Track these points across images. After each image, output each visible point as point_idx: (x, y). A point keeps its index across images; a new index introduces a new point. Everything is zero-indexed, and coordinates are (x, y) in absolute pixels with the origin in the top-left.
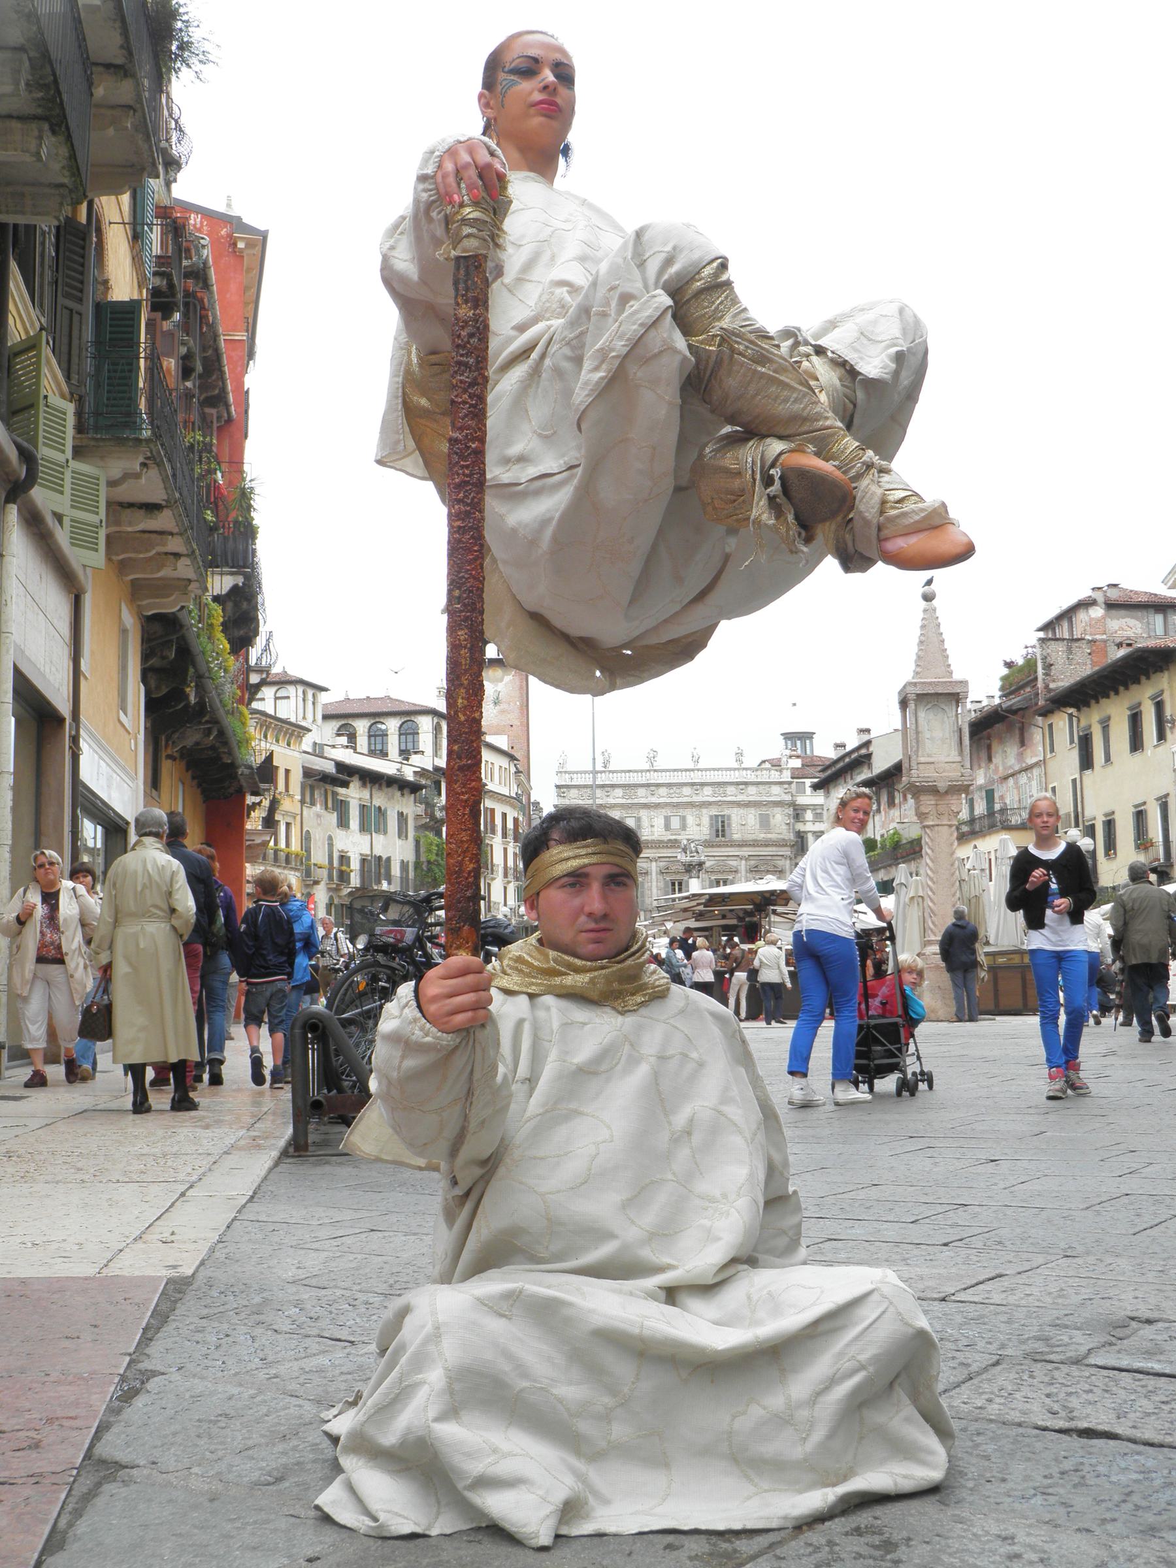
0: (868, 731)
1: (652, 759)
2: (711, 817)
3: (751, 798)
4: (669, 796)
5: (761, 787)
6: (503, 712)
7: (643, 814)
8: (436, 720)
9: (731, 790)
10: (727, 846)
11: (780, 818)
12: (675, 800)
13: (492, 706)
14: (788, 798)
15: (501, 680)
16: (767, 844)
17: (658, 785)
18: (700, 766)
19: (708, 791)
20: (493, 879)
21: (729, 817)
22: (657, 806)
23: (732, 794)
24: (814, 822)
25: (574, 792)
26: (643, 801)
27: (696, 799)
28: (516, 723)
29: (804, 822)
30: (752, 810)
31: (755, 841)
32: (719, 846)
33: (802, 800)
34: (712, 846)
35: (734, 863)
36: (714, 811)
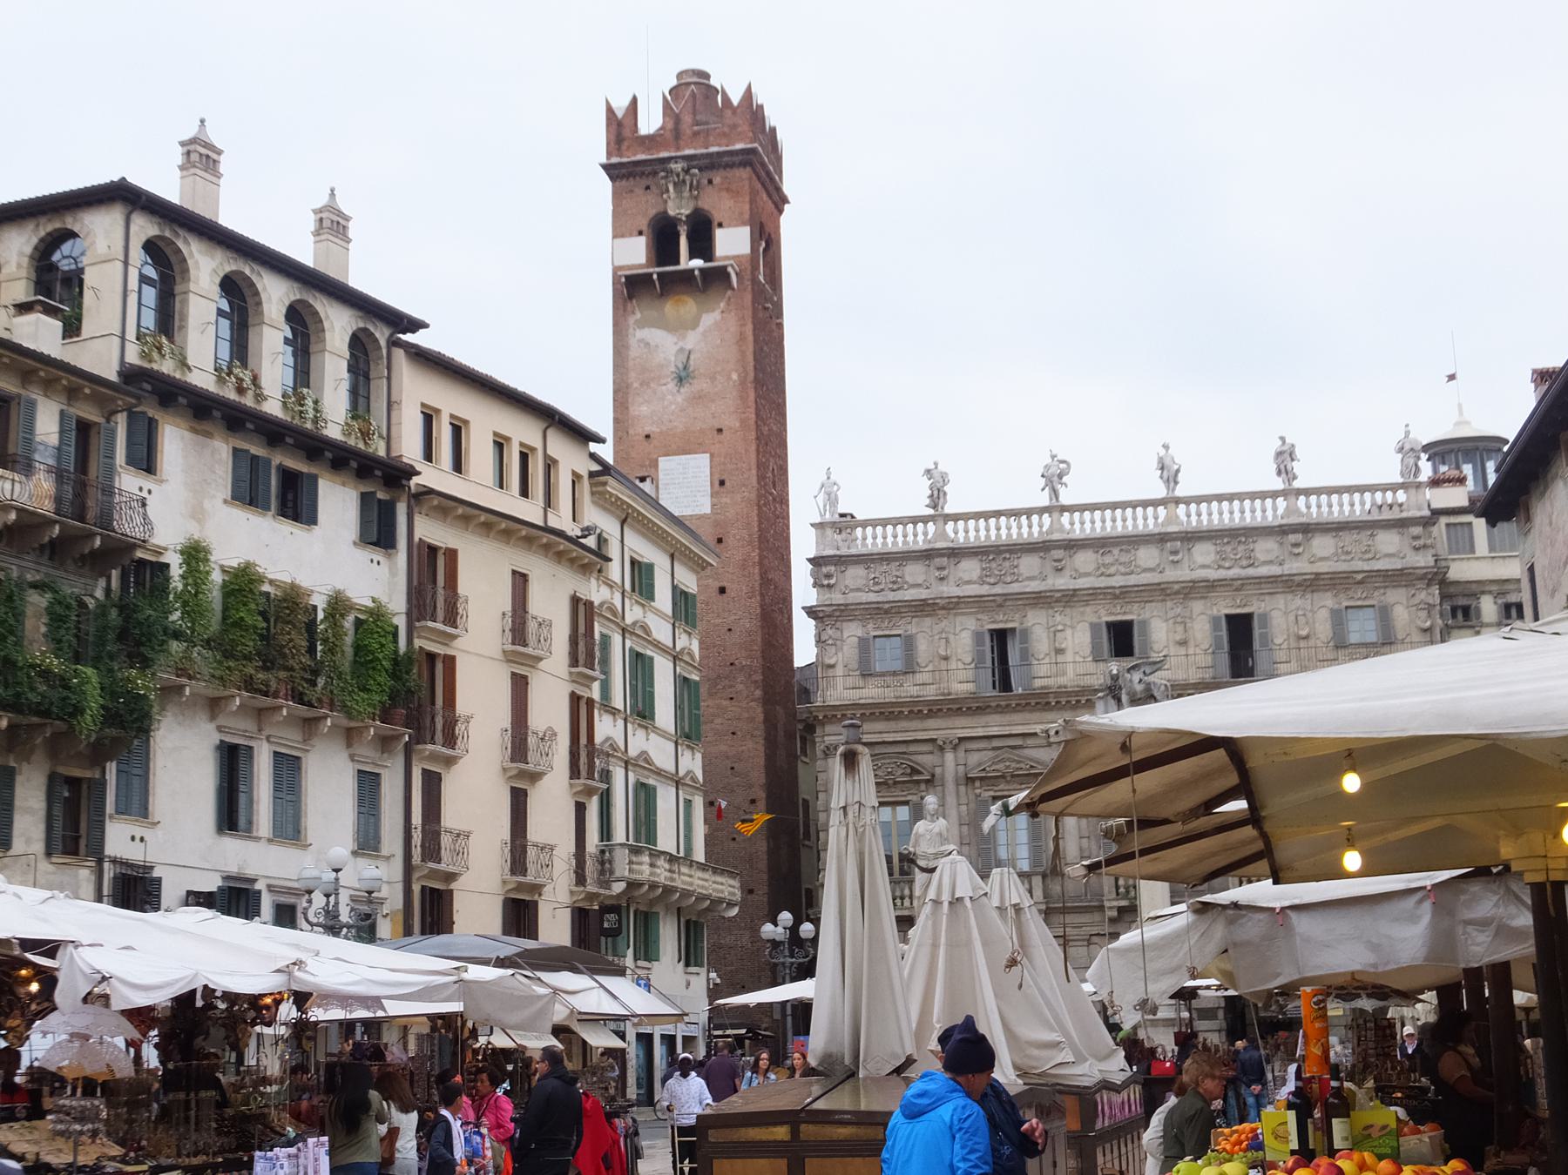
1: (1054, 478)
2: (1215, 621)
3: (1323, 567)
5: (1348, 538)
6: (698, 398)
8: (144, 228)
12: (1117, 581)
13: (672, 386)
14: (1424, 560)
15: (694, 324)
17: (1072, 545)
18: (1180, 492)
19: (1204, 553)
20: (450, 761)
21: (1264, 617)
22: (1069, 598)
26: (1034, 586)
27: (1171, 575)
28: (730, 422)
33: (1461, 571)
36: (1225, 606)
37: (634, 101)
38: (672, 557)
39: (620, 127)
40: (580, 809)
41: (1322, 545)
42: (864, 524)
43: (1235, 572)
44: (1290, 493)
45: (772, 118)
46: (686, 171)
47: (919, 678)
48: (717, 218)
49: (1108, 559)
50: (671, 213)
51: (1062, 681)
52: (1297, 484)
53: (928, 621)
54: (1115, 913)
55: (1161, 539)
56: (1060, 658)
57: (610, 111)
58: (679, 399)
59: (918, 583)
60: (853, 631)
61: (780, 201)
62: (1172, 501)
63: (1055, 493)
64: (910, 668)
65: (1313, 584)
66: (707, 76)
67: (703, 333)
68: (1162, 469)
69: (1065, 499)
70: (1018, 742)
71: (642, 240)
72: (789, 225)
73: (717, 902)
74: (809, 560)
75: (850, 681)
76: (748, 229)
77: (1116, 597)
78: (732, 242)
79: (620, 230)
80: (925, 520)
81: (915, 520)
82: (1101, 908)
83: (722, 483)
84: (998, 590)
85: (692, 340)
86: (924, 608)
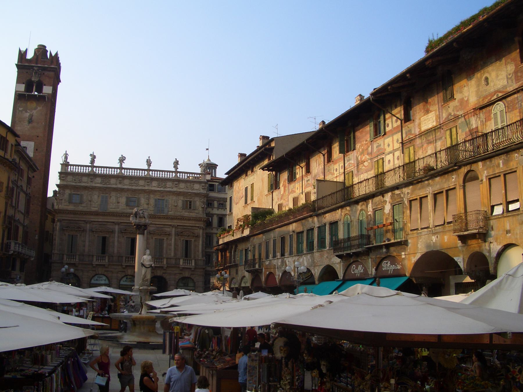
0: (267, 138)
4: (130, 184)
5: (189, 184)
7: (113, 194)
9: (169, 184)
10: (164, 218)
11: (199, 203)
12: (134, 188)
13: (27, 123)
15: (35, 109)
16: (189, 219)
18: (151, 168)
21: (166, 200)
22: (122, 190)
23: (169, 186)
24: (218, 208)
25: (70, 178)
26: (114, 186)
29: (213, 208)
30: (182, 198)
31: (183, 217)
32: (160, 218)
33: (213, 194)
34: (155, 218)
35: (168, 229)
36: (157, 197)
37: (27, 50)
38: (28, 168)
39: (22, 55)
40: (4, 231)
41: (182, 185)
42: (71, 165)
43: (162, 189)
44: (176, 172)
45: (61, 60)
46: (38, 70)
47: (83, 205)
48: (45, 83)
49: (132, 182)
50: (33, 79)
51: (118, 210)
52: (178, 170)
53: (87, 191)
54: (124, 267)
55: (145, 178)
56: (118, 204)
57: (20, 51)
58: (28, 127)
59: (86, 182)
60: (68, 192)
61: (59, 81)
62: (148, 170)
63: (121, 164)
64: (81, 203)
65: (178, 194)
66: (45, 47)
67: (36, 110)
68: (147, 162)
69: (124, 166)
70: (105, 223)
71: (24, 85)
72: (60, 87)
73: (30, 257)
74: (59, 173)
75: (65, 204)
76: (52, 87)
77: (133, 191)
78: (47, 90)
79: (18, 81)
80: (89, 166)
81: (86, 166)
82: (122, 265)
83: (37, 150)
84: (105, 186)
85: (34, 112)
86: (86, 188)
